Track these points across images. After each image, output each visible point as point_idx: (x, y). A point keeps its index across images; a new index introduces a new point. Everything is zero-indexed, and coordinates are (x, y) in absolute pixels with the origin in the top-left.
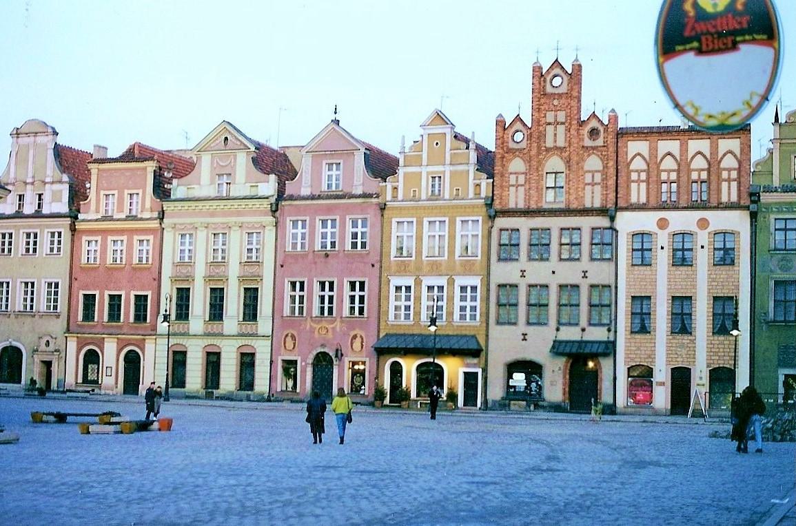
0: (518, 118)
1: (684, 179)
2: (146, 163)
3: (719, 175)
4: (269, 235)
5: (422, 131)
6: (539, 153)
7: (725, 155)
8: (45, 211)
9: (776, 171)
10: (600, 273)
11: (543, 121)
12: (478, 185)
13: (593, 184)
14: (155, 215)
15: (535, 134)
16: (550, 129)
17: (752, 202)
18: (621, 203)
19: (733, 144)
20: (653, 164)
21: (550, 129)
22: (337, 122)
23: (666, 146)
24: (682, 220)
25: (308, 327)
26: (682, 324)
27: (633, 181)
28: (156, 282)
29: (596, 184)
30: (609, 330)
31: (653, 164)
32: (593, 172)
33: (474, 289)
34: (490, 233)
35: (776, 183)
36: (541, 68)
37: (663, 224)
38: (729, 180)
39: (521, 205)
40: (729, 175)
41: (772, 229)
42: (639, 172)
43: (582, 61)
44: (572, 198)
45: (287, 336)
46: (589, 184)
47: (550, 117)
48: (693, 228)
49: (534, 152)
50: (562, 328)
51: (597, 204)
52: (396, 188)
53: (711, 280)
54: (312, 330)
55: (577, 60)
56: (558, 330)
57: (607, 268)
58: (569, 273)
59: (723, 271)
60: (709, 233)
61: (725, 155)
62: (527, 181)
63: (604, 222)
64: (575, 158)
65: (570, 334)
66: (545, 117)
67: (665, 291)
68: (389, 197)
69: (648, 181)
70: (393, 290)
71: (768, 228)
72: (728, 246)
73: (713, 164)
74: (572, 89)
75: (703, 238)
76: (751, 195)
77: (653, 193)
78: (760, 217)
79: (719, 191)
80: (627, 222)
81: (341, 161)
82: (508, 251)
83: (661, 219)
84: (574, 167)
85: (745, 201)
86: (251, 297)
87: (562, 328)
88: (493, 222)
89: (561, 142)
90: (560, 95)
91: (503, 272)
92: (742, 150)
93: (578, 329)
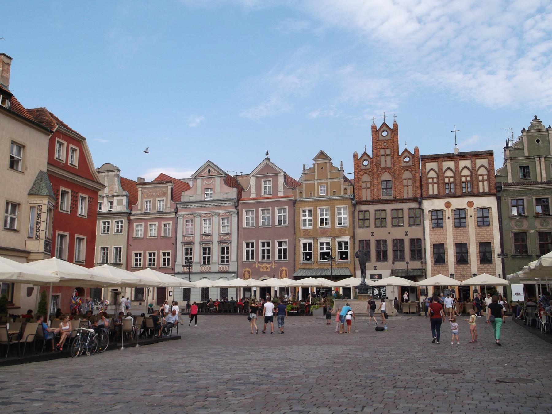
0: (365, 154)
1: (458, 180)
2: (168, 184)
3: (477, 178)
4: (234, 219)
5: (314, 162)
6: (377, 171)
7: (480, 167)
8: (114, 210)
9: (510, 175)
10: (415, 232)
12: (345, 189)
13: (407, 186)
14: (173, 210)
15: (375, 160)
16: (383, 159)
17: (497, 191)
18: (424, 195)
20: (440, 176)
21: (383, 159)
22: (268, 159)
25: (257, 266)
27: (430, 183)
28: (174, 246)
29: (409, 186)
30: (422, 263)
31: (440, 176)
32: (407, 180)
33: (346, 243)
34: (353, 212)
35: (510, 181)
36: (376, 127)
37: (448, 205)
38: (483, 181)
39: (369, 198)
40: (483, 178)
42: (433, 178)
43: (397, 122)
44: (397, 193)
45: (245, 271)
46: (406, 186)
47: (382, 152)
48: (465, 206)
49: (375, 170)
50: (395, 262)
51: (411, 196)
52: (301, 192)
53: (477, 234)
54: (259, 267)
55: (395, 121)
56: (393, 263)
58: (398, 233)
59: (484, 230)
61: (480, 167)
62: (372, 185)
63: (414, 205)
64: (397, 172)
67: (452, 240)
68: (298, 197)
69: (438, 183)
70: (302, 245)
72: (485, 215)
73: (474, 173)
74: (393, 137)
75: (471, 212)
76: (496, 188)
77: (441, 188)
78: (503, 199)
79: (478, 187)
80: (428, 205)
81: (271, 179)
82: (363, 222)
83: (447, 203)
84: (396, 176)
85: (493, 191)
86: (225, 250)
87: (395, 262)
88: (355, 208)
89: (389, 165)
90: (387, 140)
92: (489, 164)
93: (404, 263)
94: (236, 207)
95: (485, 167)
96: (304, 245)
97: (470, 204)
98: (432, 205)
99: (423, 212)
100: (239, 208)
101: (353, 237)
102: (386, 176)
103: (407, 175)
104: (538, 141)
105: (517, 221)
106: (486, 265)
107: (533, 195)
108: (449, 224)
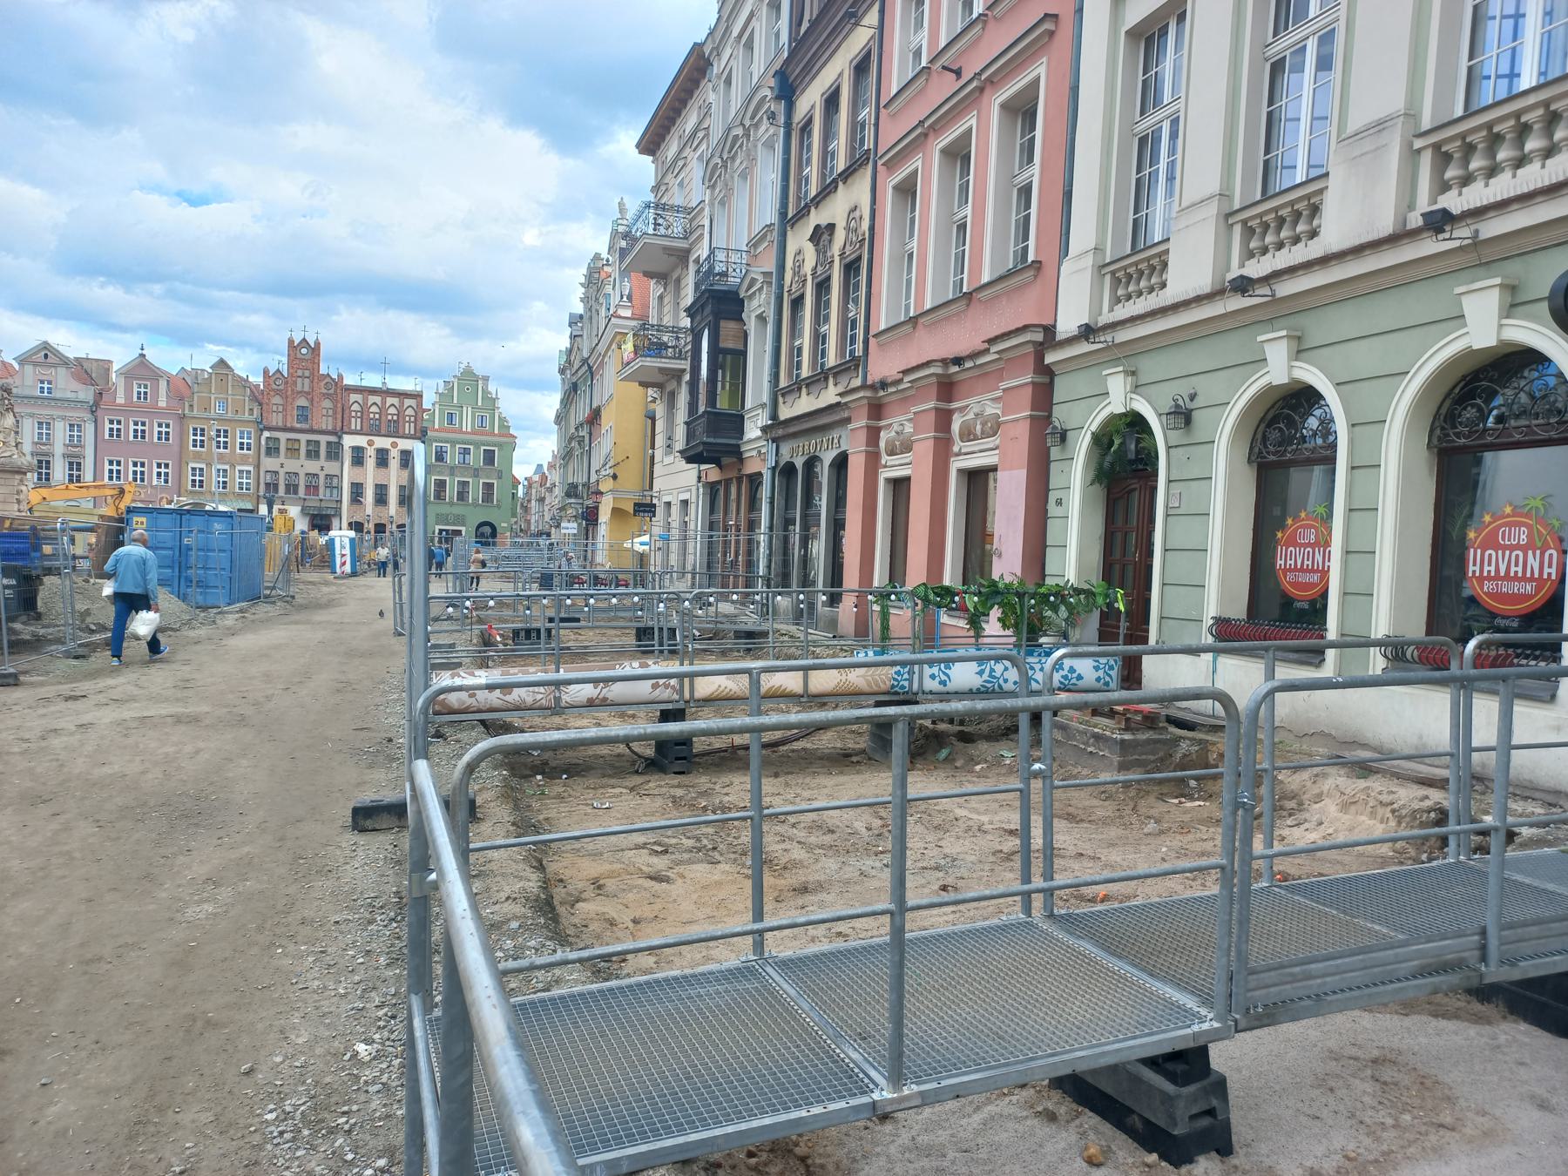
4: (89, 429)
19: (412, 402)
20: (364, 410)
22: (143, 356)
23: (372, 399)
24: (383, 442)
31: (364, 410)
37: (370, 443)
47: (300, 373)
57: (336, 465)
62: (285, 409)
65: (313, 502)
80: (349, 441)
82: (272, 450)
89: (306, 389)
91: (269, 463)
94: (92, 412)
96: (194, 469)
97: (394, 445)
100: (99, 413)
101: (258, 467)
102: (302, 402)
103: (327, 403)
108: (370, 462)
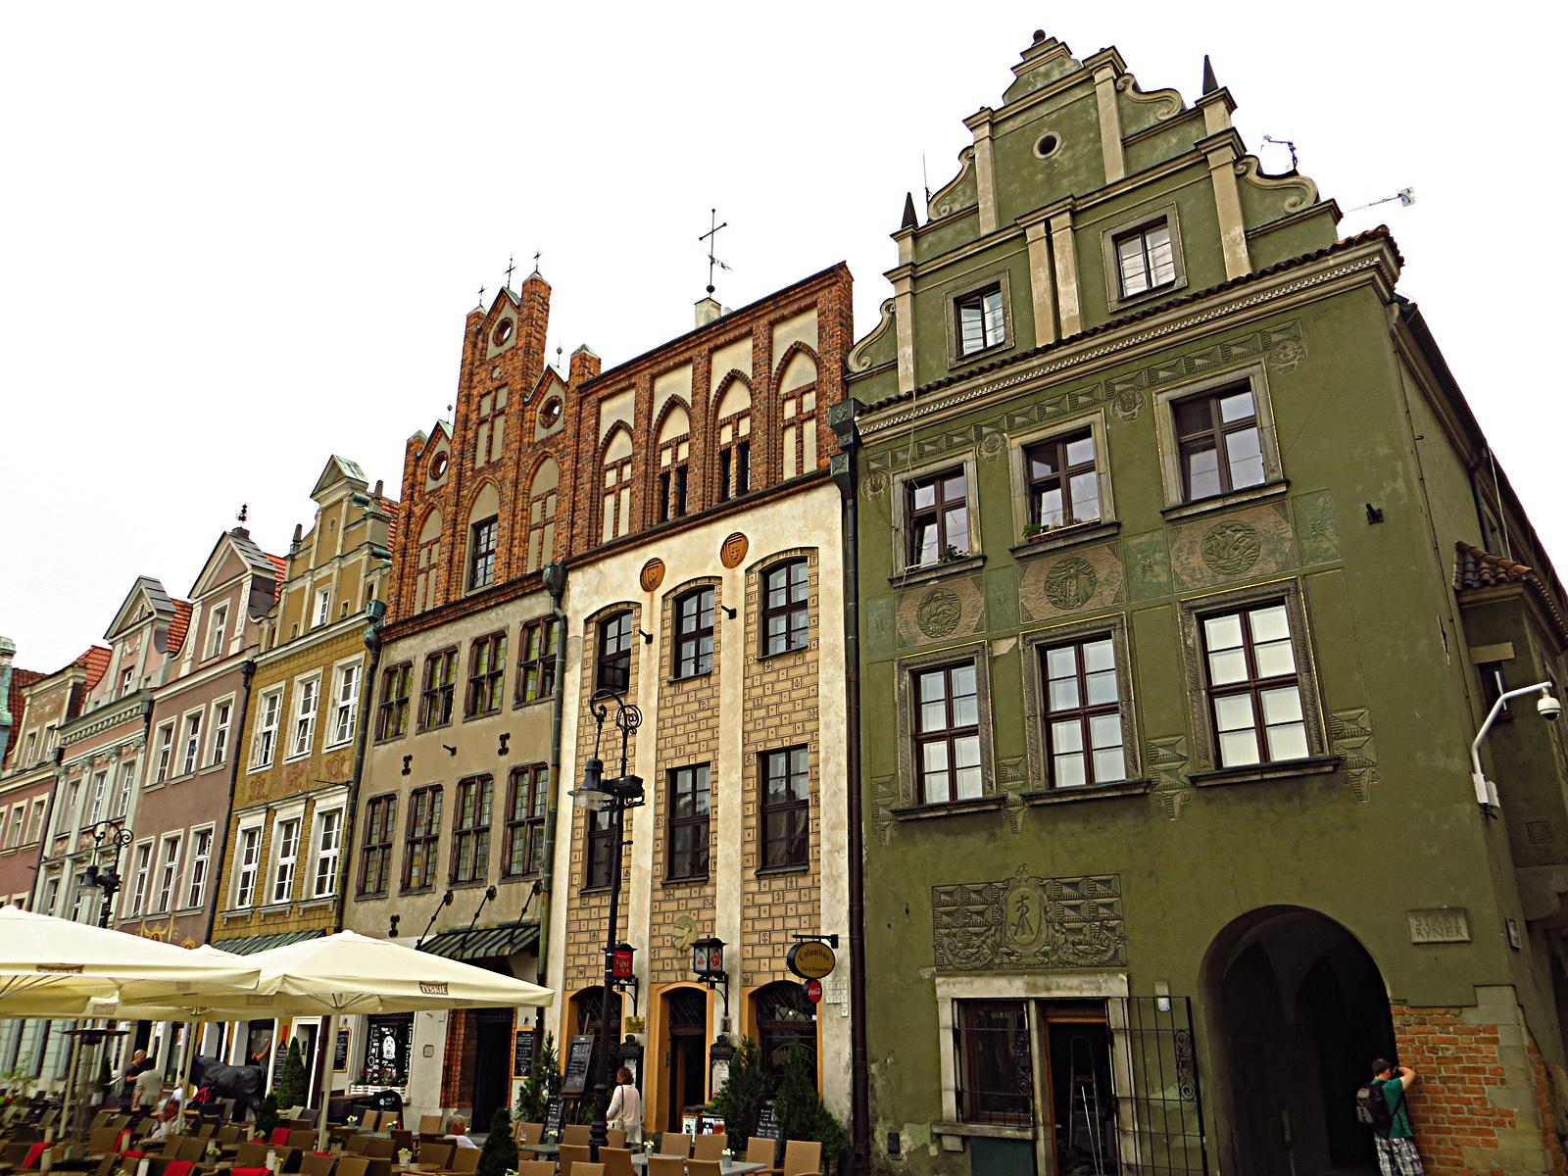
9: (906, 352)
11: (474, 416)
22: (242, 534)
24: (689, 555)
26: (687, 855)
38: (799, 422)
41: (897, 516)
48: (714, 567)
53: (751, 704)
55: (536, 272)
60: (749, 571)
63: (539, 605)
66: (479, 408)
71: (884, 513)
79: (775, 456)
80: (589, 592)
95: (808, 351)
98: (597, 591)
99: (565, 631)
104: (1047, 145)
105: (931, 598)
106: (779, 884)
107: (1012, 428)
